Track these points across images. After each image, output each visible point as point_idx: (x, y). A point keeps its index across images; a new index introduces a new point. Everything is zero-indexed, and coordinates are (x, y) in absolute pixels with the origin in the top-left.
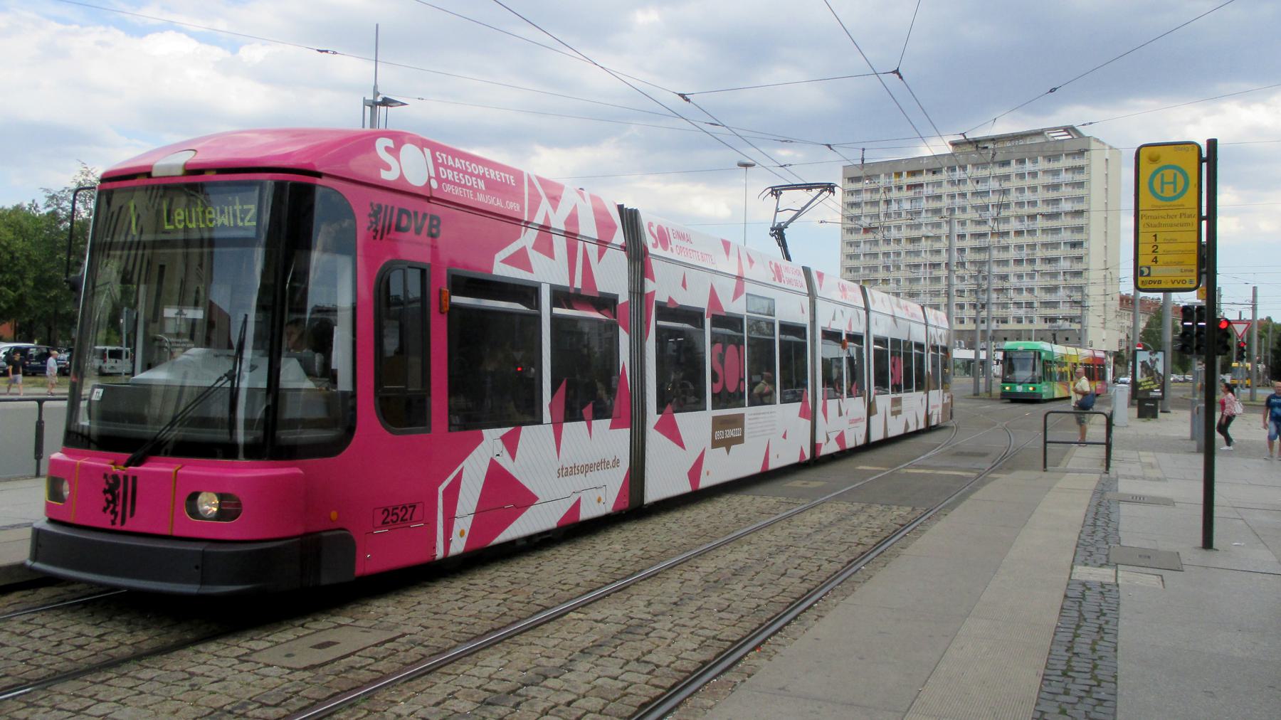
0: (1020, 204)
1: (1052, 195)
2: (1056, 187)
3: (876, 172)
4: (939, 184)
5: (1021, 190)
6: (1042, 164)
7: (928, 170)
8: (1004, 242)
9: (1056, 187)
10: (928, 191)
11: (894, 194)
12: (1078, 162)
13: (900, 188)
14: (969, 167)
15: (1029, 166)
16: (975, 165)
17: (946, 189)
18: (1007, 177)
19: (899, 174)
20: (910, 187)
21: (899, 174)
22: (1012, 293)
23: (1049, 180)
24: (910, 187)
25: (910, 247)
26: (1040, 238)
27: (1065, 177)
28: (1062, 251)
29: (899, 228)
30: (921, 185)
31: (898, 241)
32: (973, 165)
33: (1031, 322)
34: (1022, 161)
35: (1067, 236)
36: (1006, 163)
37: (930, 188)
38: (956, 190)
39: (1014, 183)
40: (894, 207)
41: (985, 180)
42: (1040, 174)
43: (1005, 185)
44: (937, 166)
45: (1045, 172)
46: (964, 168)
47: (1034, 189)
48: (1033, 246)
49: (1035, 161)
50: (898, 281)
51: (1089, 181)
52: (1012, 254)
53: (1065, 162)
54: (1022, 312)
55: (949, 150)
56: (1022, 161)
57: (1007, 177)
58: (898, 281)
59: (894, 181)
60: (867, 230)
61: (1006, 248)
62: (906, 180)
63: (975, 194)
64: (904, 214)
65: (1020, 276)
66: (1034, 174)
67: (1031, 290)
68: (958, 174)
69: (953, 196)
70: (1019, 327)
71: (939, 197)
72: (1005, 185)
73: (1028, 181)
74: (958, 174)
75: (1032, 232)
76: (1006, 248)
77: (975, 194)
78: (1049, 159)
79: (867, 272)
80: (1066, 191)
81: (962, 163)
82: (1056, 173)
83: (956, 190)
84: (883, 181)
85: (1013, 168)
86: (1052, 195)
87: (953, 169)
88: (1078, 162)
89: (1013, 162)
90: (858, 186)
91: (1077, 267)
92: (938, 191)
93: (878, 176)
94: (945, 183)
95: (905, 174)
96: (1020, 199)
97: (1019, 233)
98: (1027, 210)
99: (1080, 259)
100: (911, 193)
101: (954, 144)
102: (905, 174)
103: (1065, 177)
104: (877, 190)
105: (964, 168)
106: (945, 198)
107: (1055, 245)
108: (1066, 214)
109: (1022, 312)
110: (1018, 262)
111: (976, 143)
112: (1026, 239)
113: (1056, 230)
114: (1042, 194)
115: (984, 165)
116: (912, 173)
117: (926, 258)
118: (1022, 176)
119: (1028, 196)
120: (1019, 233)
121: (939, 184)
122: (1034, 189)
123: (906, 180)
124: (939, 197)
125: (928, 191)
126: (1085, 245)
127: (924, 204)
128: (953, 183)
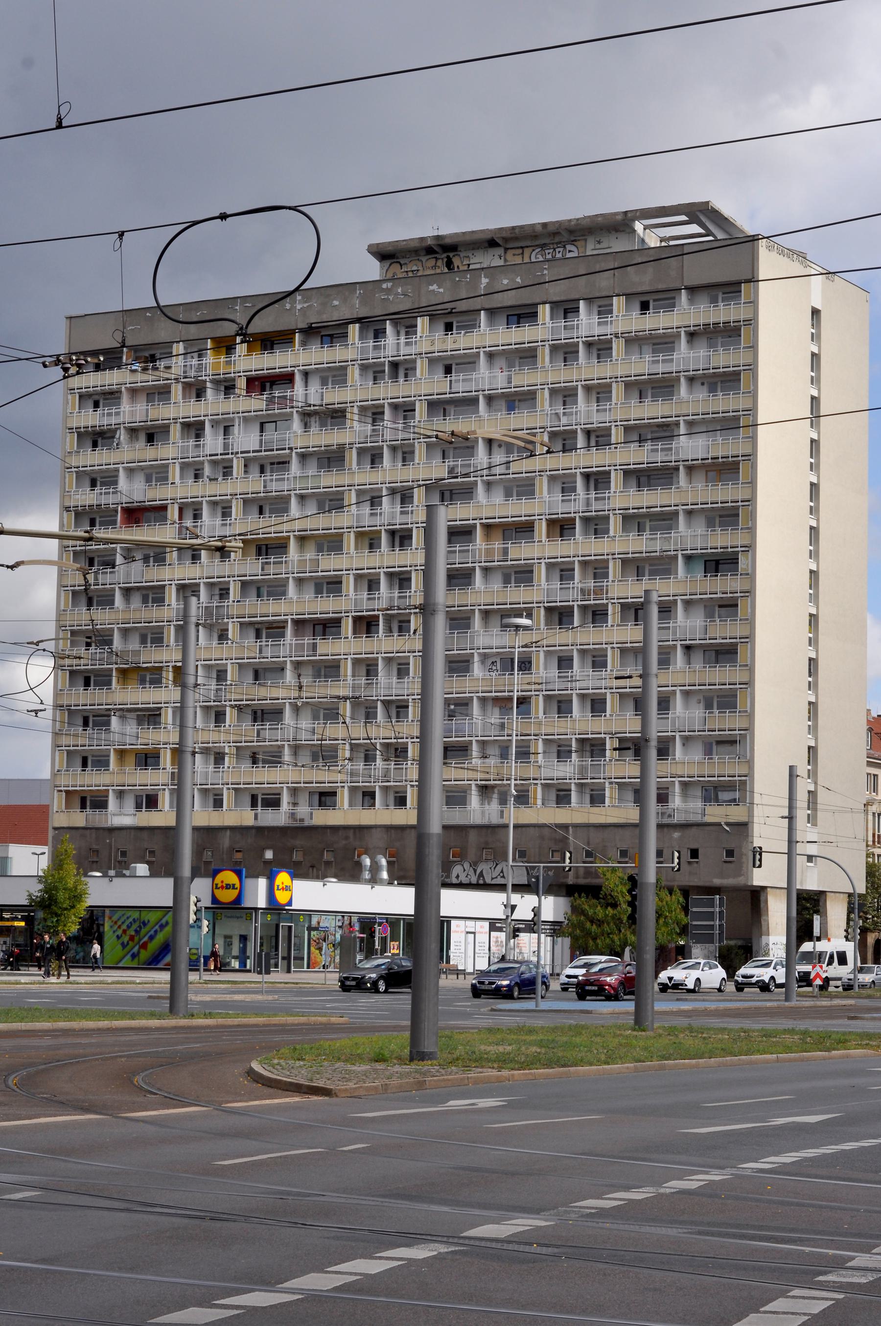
1: (653, 410)
4: (336, 375)
5: (565, 395)
6: (625, 319)
8: (521, 552)
15: (587, 324)
18: (526, 356)
23: (643, 365)
25: (252, 567)
26: (620, 543)
27: (687, 357)
30: (287, 379)
36: (523, 315)
37: (315, 387)
38: (388, 391)
42: (618, 347)
43: (524, 379)
45: (634, 341)
47: (599, 392)
52: (543, 589)
53: (687, 313)
57: (526, 356)
61: (523, 574)
66: (600, 348)
68: (393, 344)
69: (375, 414)
71: (335, 416)
72: (524, 379)
73: (586, 369)
75: (596, 525)
76: (523, 574)
80: (690, 401)
82: (662, 343)
83: (388, 391)
85: (545, 328)
86: (653, 410)
89: (544, 311)
92: (334, 396)
98: (585, 458)
100: (257, 403)
103: (687, 357)
106: (353, 414)
107: (660, 566)
108: (691, 469)
111: (444, 251)
112: (581, 546)
113: (664, 520)
114: (624, 409)
117: (298, 603)
119: (585, 413)
120: (561, 527)
121: (336, 375)
122: (599, 392)
124: (335, 416)
127: (296, 435)
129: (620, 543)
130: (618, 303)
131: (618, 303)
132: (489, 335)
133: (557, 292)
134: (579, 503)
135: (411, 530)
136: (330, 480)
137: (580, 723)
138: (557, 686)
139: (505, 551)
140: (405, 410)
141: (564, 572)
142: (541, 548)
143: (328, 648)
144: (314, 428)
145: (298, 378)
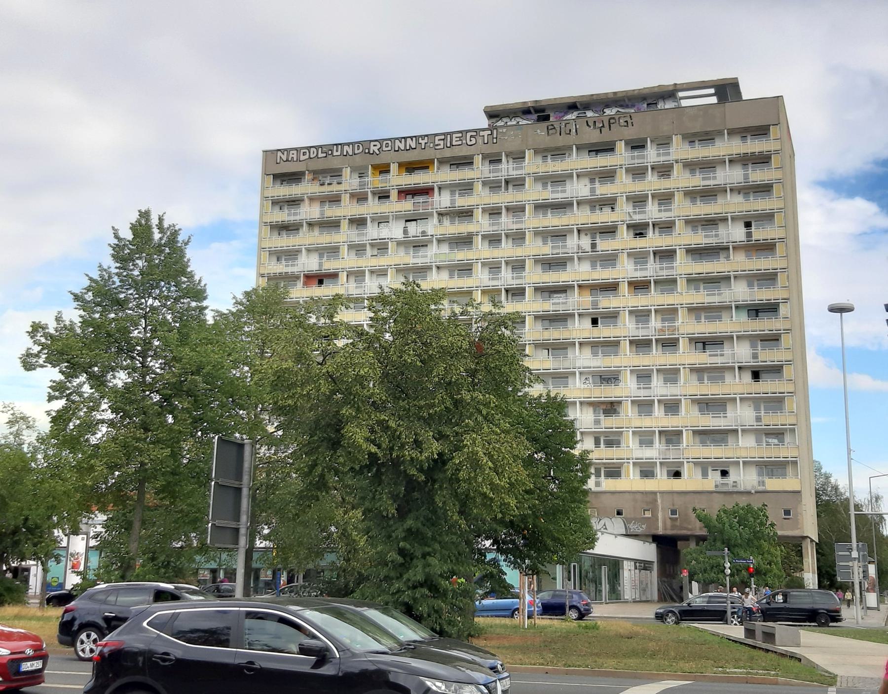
0: (639, 230)
2: (708, 194)
3: (334, 163)
4: (466, 188)
5: (639, 201)
6: (680, 150)
7: (442, 162)
8: (608, 302)
9: (708, 194)
10: (443, 200)
11: (372, 207)
12: (755, 146)
13: (383, 196)
14: (528, 154)
15: (652, 155)
16: (543, 152)
17: (481, 197)
18: (608, 175)
19: (384, 169)
20: (406, 193)
22: (628, 412)
23: (697, 181)
24: (406, 193)
26: (684, 296)
28: (734, 323)
30: (426, 191)
32: (537, 152)
33: (677, 474)
34: (637, 145)
35: (740, 292)
39: (624, 185)
40: (373, 232)
41: (559, 180)
43: (604, 190)
44: (464, 151)
46: (518, 157)
48: (669, 313)
49: (664, 143)
52: (627, 328)
54: (654, 452)
56: (637, 145)
57: (608, 175)
59: (374, 181)
62: (397, 179)
63: (541, 207)
66: (664, 171)
67: (672, 406)
68: (507, 169)
69: (494, 212)
70: (649, 485)
71: (466, 214)
72: (604, 190)
73: (652, 183)
74: (507, 169)
77: (541, 207)
78: (691, 138)
80: (734, 204)
82: (707, 166)
84: (350, 182)
85: (622, 156)
88: (755, 146)
91: (768, 356)
92: (462, 202)
93: (336, 173)
94: (478, 187)
95: (394, 168)
96: (638, 218)
97: (639, 286)
98: (654, 240)
99: (773, 339)
100: (407, 205)
102: (394, 168)
103: (731, 175)
104: (335, 200)
105: (518, 157)
109: (654, 452)
110: (641, 345)
112: (654, 299)
115: (559, 152)
116: (410, 167)
118: (638, 173)
120: (639, 286)
123: (397, 179)
124: (466, 214)
125: (443, 200)
126: (783, 310)
128: (493, 186)
129: (684, 296)
130: (676, 140)
131: (676, 140)
133: (631, 133)
134: (652, 270)
135: (524, 289)
136: (461, 255)
137: (659, 419)
138: (642, 394)
140: (517, 210)
142: (625, 300)
144: (446, 221)
145: (436, 190)
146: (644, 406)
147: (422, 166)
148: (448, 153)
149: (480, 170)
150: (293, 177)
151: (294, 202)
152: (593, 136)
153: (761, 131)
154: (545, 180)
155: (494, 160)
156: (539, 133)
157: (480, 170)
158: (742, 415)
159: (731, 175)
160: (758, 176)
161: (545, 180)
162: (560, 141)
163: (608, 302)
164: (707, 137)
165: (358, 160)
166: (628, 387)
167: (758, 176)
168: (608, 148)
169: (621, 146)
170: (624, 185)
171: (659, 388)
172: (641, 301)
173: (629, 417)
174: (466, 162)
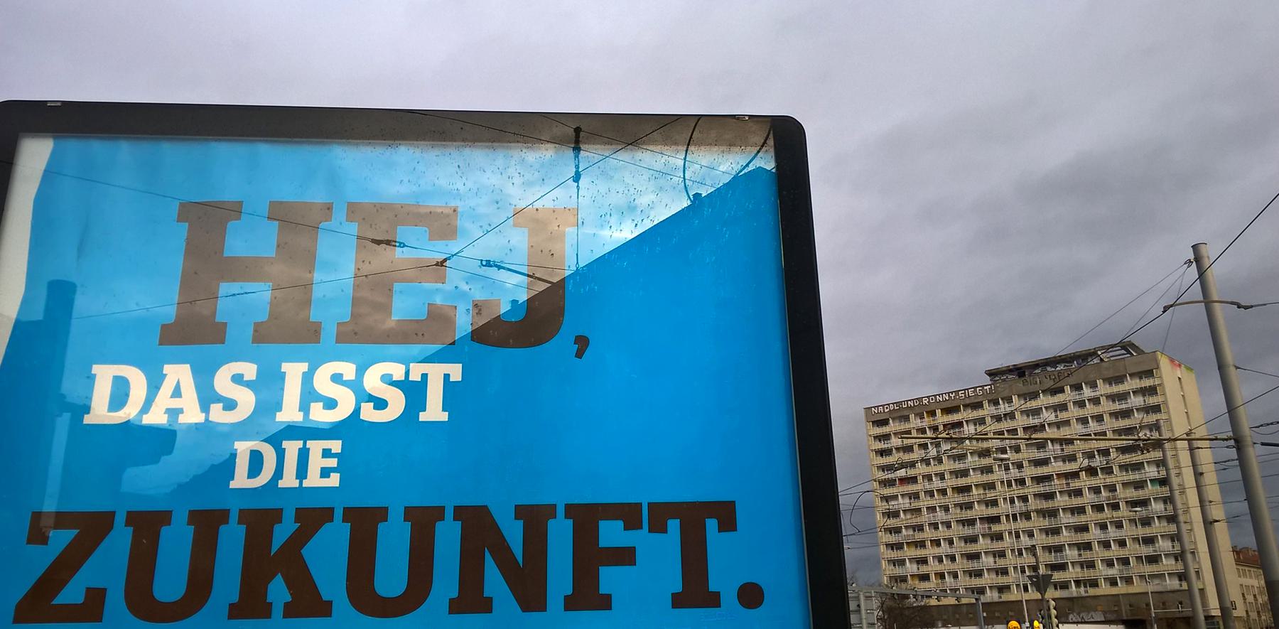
2: (1126, 414)
6: (1103, 389)
7: (966, 406)
8: (1075, 484)
12: (1147, 383)
14: (1015, 398)
15: (1087, 392)
18: (1063, 407)
19: (932, 413)
21: (932, 413)
29: (941, 476)
31: (943, 492)
34: (1077, 387)
39: (1074, 412)
43: (1063, 416)
46: (1009, 400)
49: (1093, 385)
50: (951, 542)
51: (1165, 403)
53: (1131, 384)
55: (987, 380)
56: (1077, 387)
57: (1063, 407)
58: (951, 542)
60: (903, 481)
62: (941, 419)
64: (944, 459)
65: (1103, 527)
66: (1095, 401)
68: (1004, 408)
72: (1063, 416)
73: (1090, 409)
74: (1004, 408)
76: (1078, 493)
78: (1110, 381)
79: (911, 532)
81: (1006, 394)
82: (1122, 397)
84: (915, 422)
85: (1068, 395)
87: (996, 403)
88: (1147, 383)
89: (1067, 389)
90: (885, 430)
93: (907, 419)
95: (938, 412)
101: (992, 374)
102: (938, 412)
103: (1136, 401)
111: (1019, 371)
115: (1034, 396)
116: (947, 411)
117: (979, 510)
118: (1081, 404)
122: (1099, 418)
123: (941, 419)
125: (969, 429)
132: (1044, 400)
133: (1073, 380)
138: (1102, 537)
139: (1068, 484)
141: (1096, 490)
143: (996, 528)
146: (1106, 545)
147: (955, 409)
148: (968, 402)
149: (988, 410)
150: (884, 423)
151: (886, 437)
152: (1049, 384)
153: (1149, 373)
154: (1028, 413)
155: (995, 403)
156: (1020, 386)
157: (988, 410)
158: (1164, 545)
159: (1136, 401)
160: (1152, 400)
161: (1028, 413)
162: (1032, 388)
163: (1075, 484)
164: (1119, 379)
165: (918, 411)
166: (1094, 534)
167: (1152, 400)
168: (1062, 391)
169: (1067, 389)
170: (1074, 412)
171: (1112, 533)
172: (1094, 482)
173: (1098, 553)
174: (979, 405)
